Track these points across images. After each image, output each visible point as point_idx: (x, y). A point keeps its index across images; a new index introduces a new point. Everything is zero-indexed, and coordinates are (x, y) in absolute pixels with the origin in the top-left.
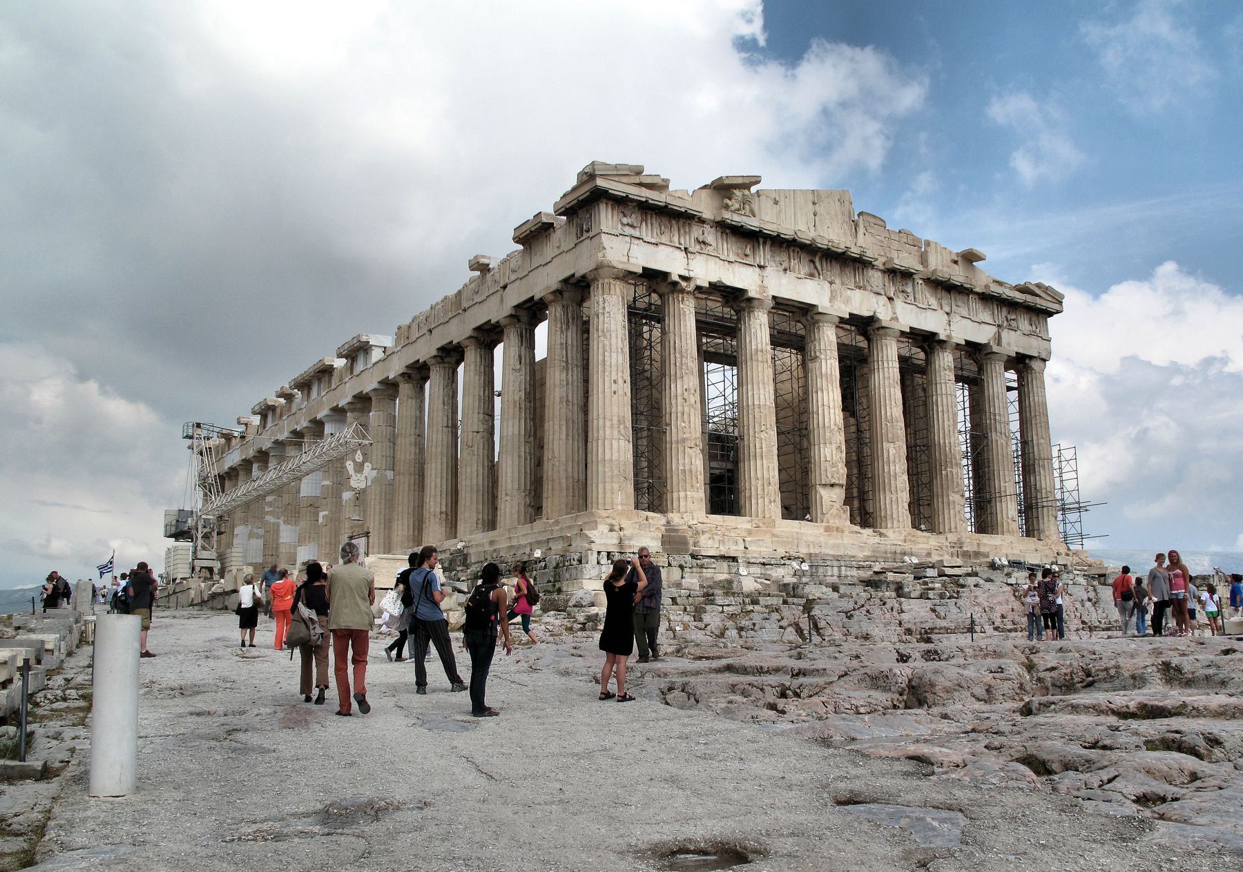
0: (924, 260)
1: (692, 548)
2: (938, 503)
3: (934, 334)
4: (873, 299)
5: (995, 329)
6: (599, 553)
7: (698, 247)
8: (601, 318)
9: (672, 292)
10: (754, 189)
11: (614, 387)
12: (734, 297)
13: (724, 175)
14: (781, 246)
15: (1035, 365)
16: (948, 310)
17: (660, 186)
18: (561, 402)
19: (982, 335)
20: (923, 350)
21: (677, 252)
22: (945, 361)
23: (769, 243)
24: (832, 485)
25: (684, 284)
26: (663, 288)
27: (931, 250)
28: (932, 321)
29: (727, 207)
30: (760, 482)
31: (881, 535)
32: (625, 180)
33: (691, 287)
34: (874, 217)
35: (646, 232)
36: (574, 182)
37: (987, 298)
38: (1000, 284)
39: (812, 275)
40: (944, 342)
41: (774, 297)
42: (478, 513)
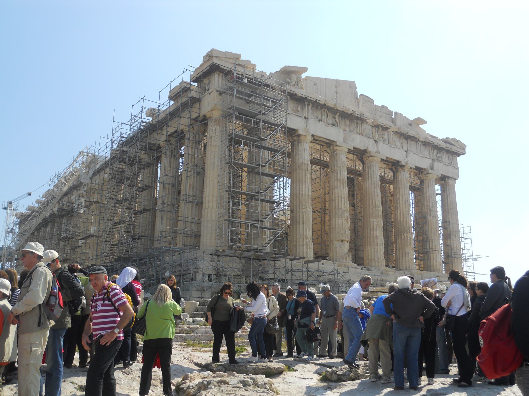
0: (393, 121)
5: (431, 161)
8: (213, 138)
10: (303, 76)
13: (287, 65)
16: (405, 148)
18: (190, 188)
19: (424, 164)
23: (311, 105)
24: (342, 241)
28: (397, 155)
29: (289, 83)
34: (368, 97)
36: (201, 62)
40: (404, 166)
41: (313, 135)
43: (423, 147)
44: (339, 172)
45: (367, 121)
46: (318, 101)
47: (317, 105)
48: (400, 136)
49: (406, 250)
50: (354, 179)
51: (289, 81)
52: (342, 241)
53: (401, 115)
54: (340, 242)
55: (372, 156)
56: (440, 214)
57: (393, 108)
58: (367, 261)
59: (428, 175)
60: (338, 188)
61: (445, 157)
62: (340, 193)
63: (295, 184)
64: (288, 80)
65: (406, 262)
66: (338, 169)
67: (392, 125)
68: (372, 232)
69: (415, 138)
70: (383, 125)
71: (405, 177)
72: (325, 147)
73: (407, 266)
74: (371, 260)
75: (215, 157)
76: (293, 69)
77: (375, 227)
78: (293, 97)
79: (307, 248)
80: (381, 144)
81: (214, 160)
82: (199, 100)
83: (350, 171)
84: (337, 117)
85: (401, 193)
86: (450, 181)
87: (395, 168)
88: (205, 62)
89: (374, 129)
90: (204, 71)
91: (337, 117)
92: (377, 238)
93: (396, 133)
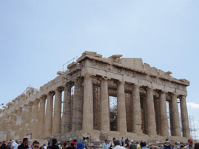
0: (158, 74)
2: (162, 129)
4: (148, 82)
10: (121, 58)
11: (89, 101)
12: (116, 81)
15: (183, 97)
17: (99, 56)
18: (77, 105)
19: (172, 91)
20: (159, 94)
22: (164, 96)
26: (101, 79)
27: (160, 72)
28: (160, 87)
29: (115, 62)
30: (122, 124)
31: (150, 136)
32: (93, 55)
35: (97, 66)
37: (172, 82)
38: (176, 79)
39: (134, 77)
41: (125, 82)
43: (171, 84)
47: (127, 70)
48: (161, 80)
49: (166, 128)
50: (143, 98)
56: (180, 111)
64: (115, 60)
66: (136, 95)
68: (151, 121)
77: (152, 118)
80: (153, 83)
82: (80, 70)
86: (183, 97)
93: (159, 78)
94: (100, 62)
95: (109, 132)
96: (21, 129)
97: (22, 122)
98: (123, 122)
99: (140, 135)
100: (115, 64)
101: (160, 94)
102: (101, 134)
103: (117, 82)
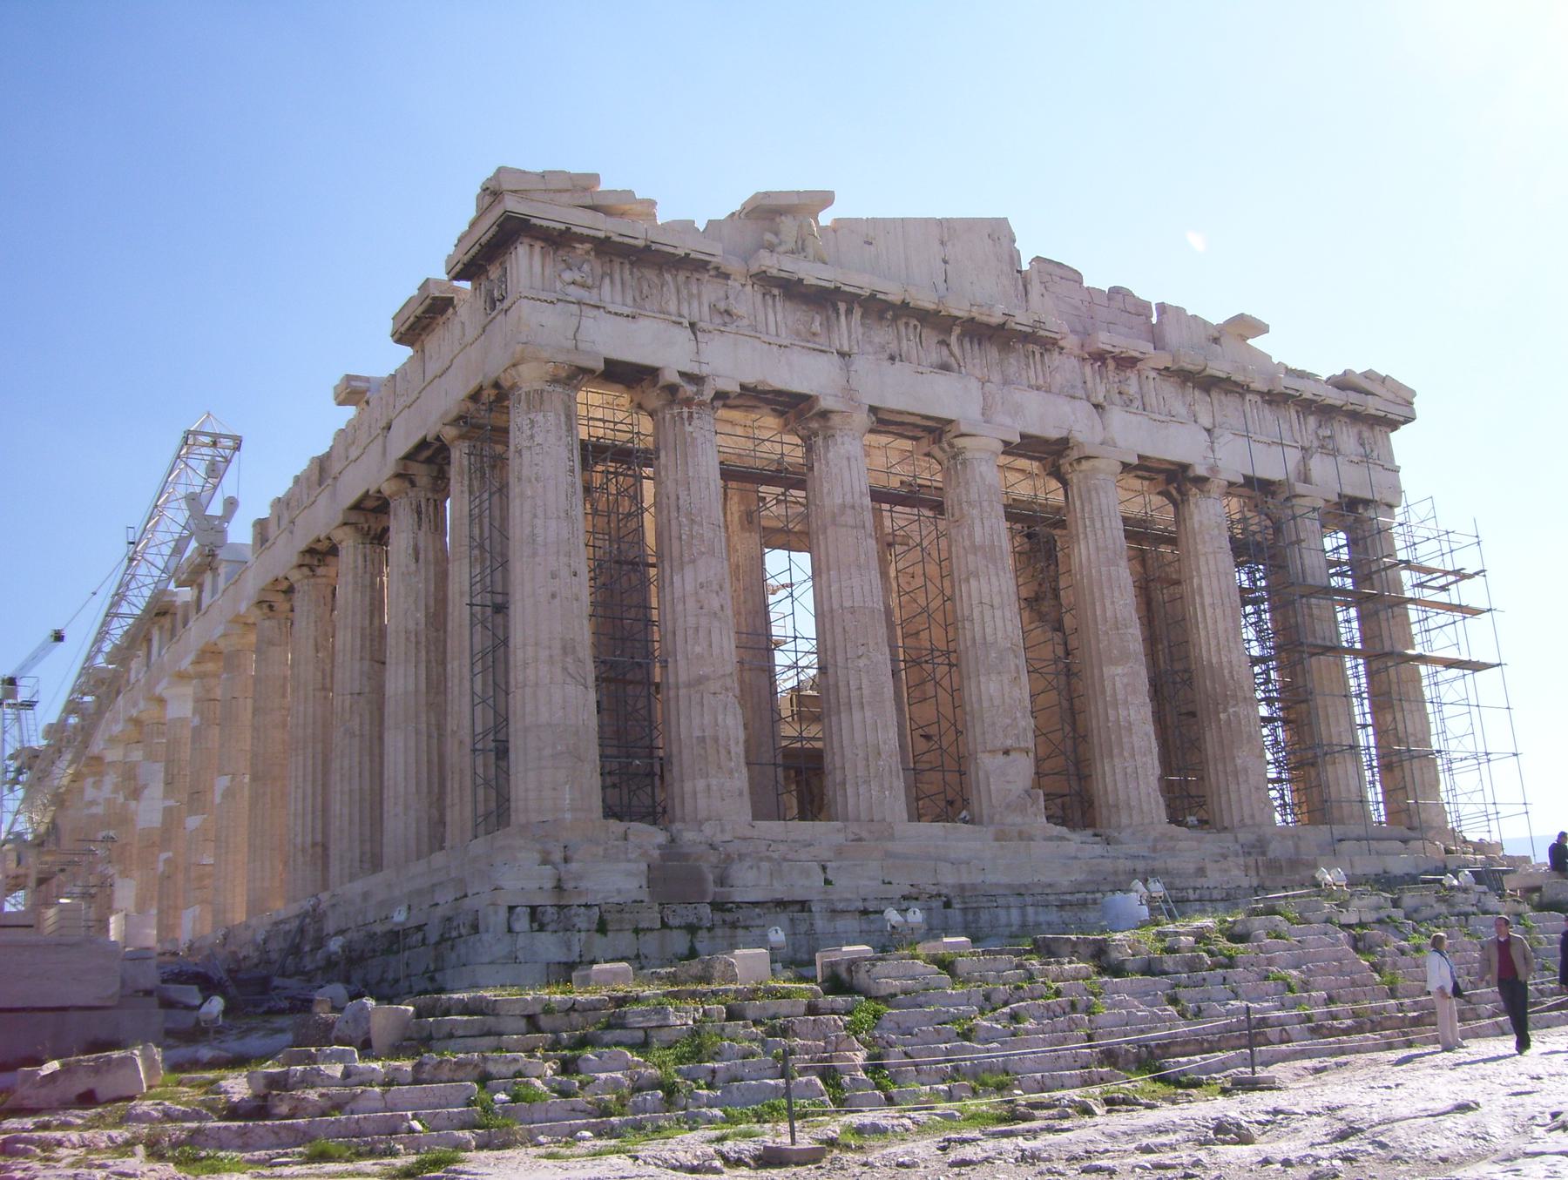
0: (1156, 337)
1: (712, 888)
3: (1184, 467)
5: (1298, 454)
6: (511, 909)
7: (718, 320)
8: (526, 455)
9: (671, 403)
10: (825, 218)
14: (881, 318)
21: (676, 330)
23: (857, 313)
25: (689, 389)
26: (654, 399)
29: (771, 248)
33: (708, 395)
34: (1060, 265)
36: (471, 212)
38: (1302, 375)
39: (945, 367)
40: (1204, 480)
41: (873, 410)
42: (362, 842)
43: (1267, 412)
44: (977, 521)
45: (1061, 343)
46: (880, 296)
47: (876, 308)
48: (1184, 382)
49: (1239, 761)
50: (1040, 538)
51: (775, 240)
52: (1006, 752)
53: (1179, 311)
54: (1000, 759)
55: (1088, 458)
57: (1150, 292)
58: (1104, 811)
59: (1294, 501)
60: (977, 576)
61: (1347, 438)
62: (985, 591)
63: (824, 577)
64: (769, 237)
65: (1240, 801)
67: (1148, 348)
68: (1110, 712)
69: (1236, 383)
70: (1117, 350)
71: (1212, 517)
72: (924, 442)
73: (1247, 812)
74: (1116, 806)
75: (535, 516)
76: (783, 202)
77: (1120, 697)
78: (792, 290)
79: (882, 786)
80: (1116, 416)
81: (534, 527)
83: (1016, 513)
84: (953, 339)
85: (1204, 569)
87: (1179, 490)
88: (482, 213)
89: (1088, 369)
90: (483, 241)
91: (953, 339)
92: (1129, 729)
93: (1166, 372)
94: (637, 256)
95: (748, 832)
96: (168, 861)
97: (171, 803)
98: (869, 743)
99: (1022, 836)
100: (769, 262)
101: (1179, 503)
102: (672, 850)
103: (800, 416)
